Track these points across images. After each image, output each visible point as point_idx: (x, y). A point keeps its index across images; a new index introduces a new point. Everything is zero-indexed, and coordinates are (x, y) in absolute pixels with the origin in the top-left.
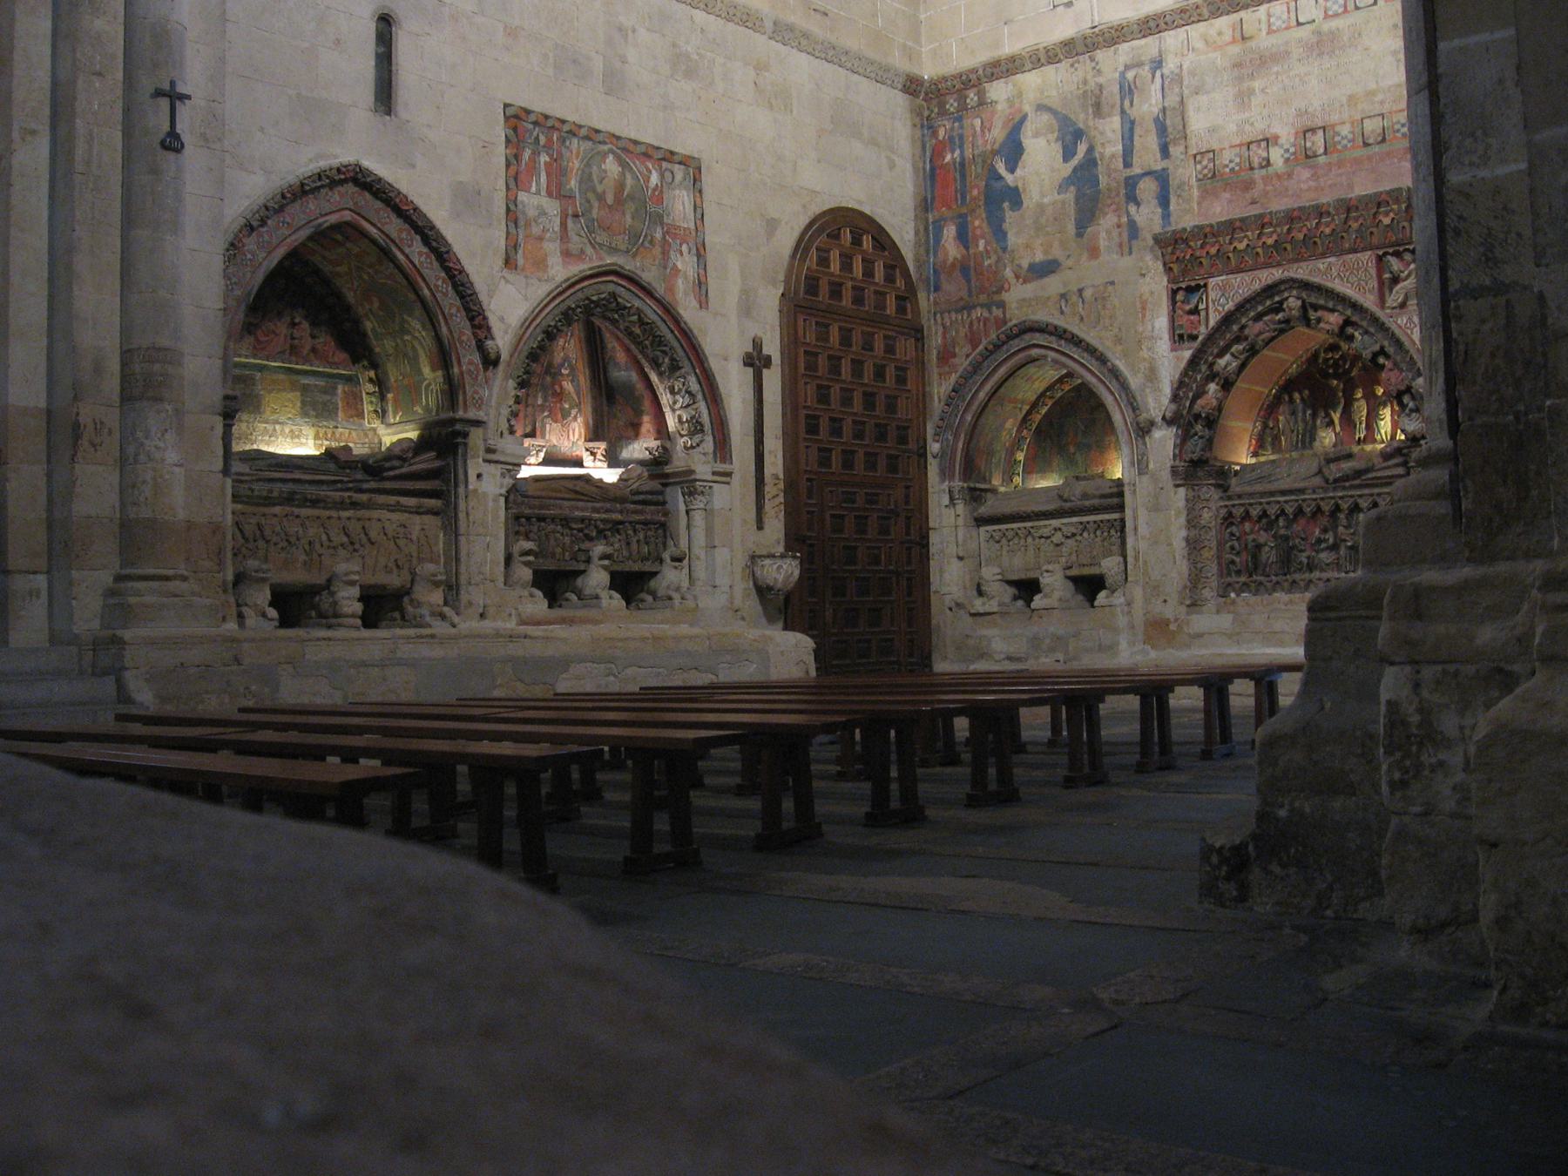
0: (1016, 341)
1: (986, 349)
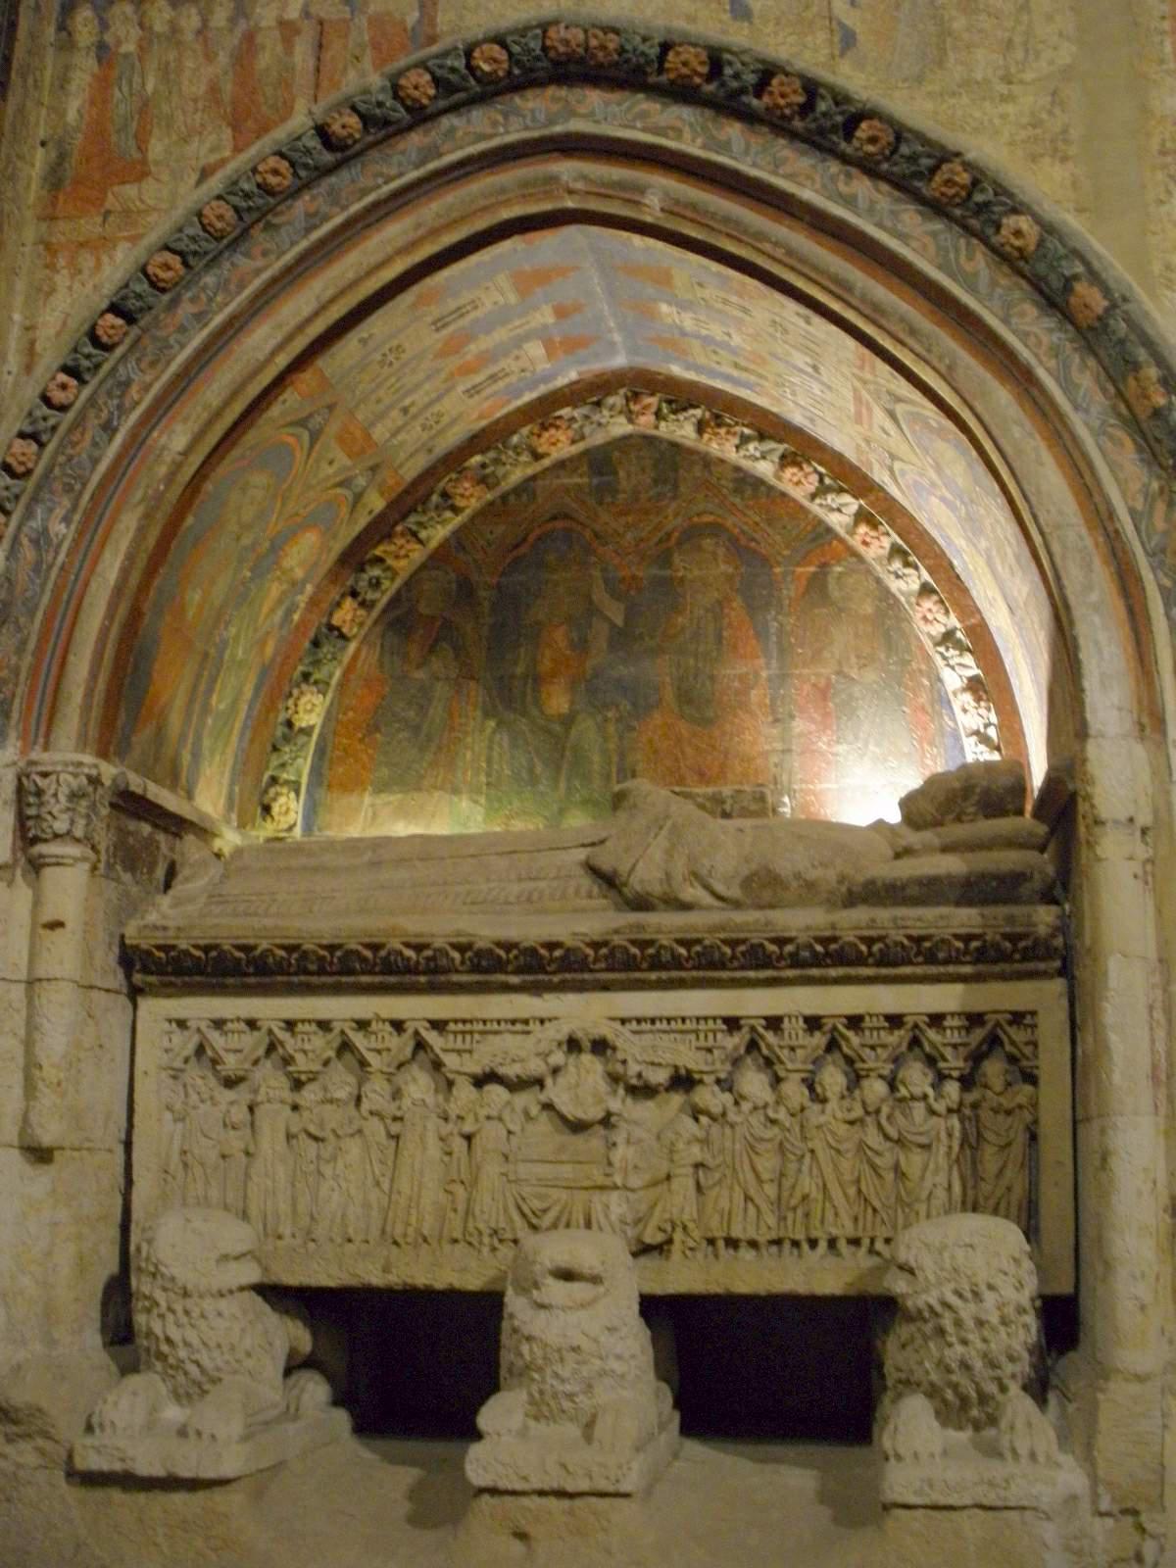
0: (479, 118)
1: (322, 132)
